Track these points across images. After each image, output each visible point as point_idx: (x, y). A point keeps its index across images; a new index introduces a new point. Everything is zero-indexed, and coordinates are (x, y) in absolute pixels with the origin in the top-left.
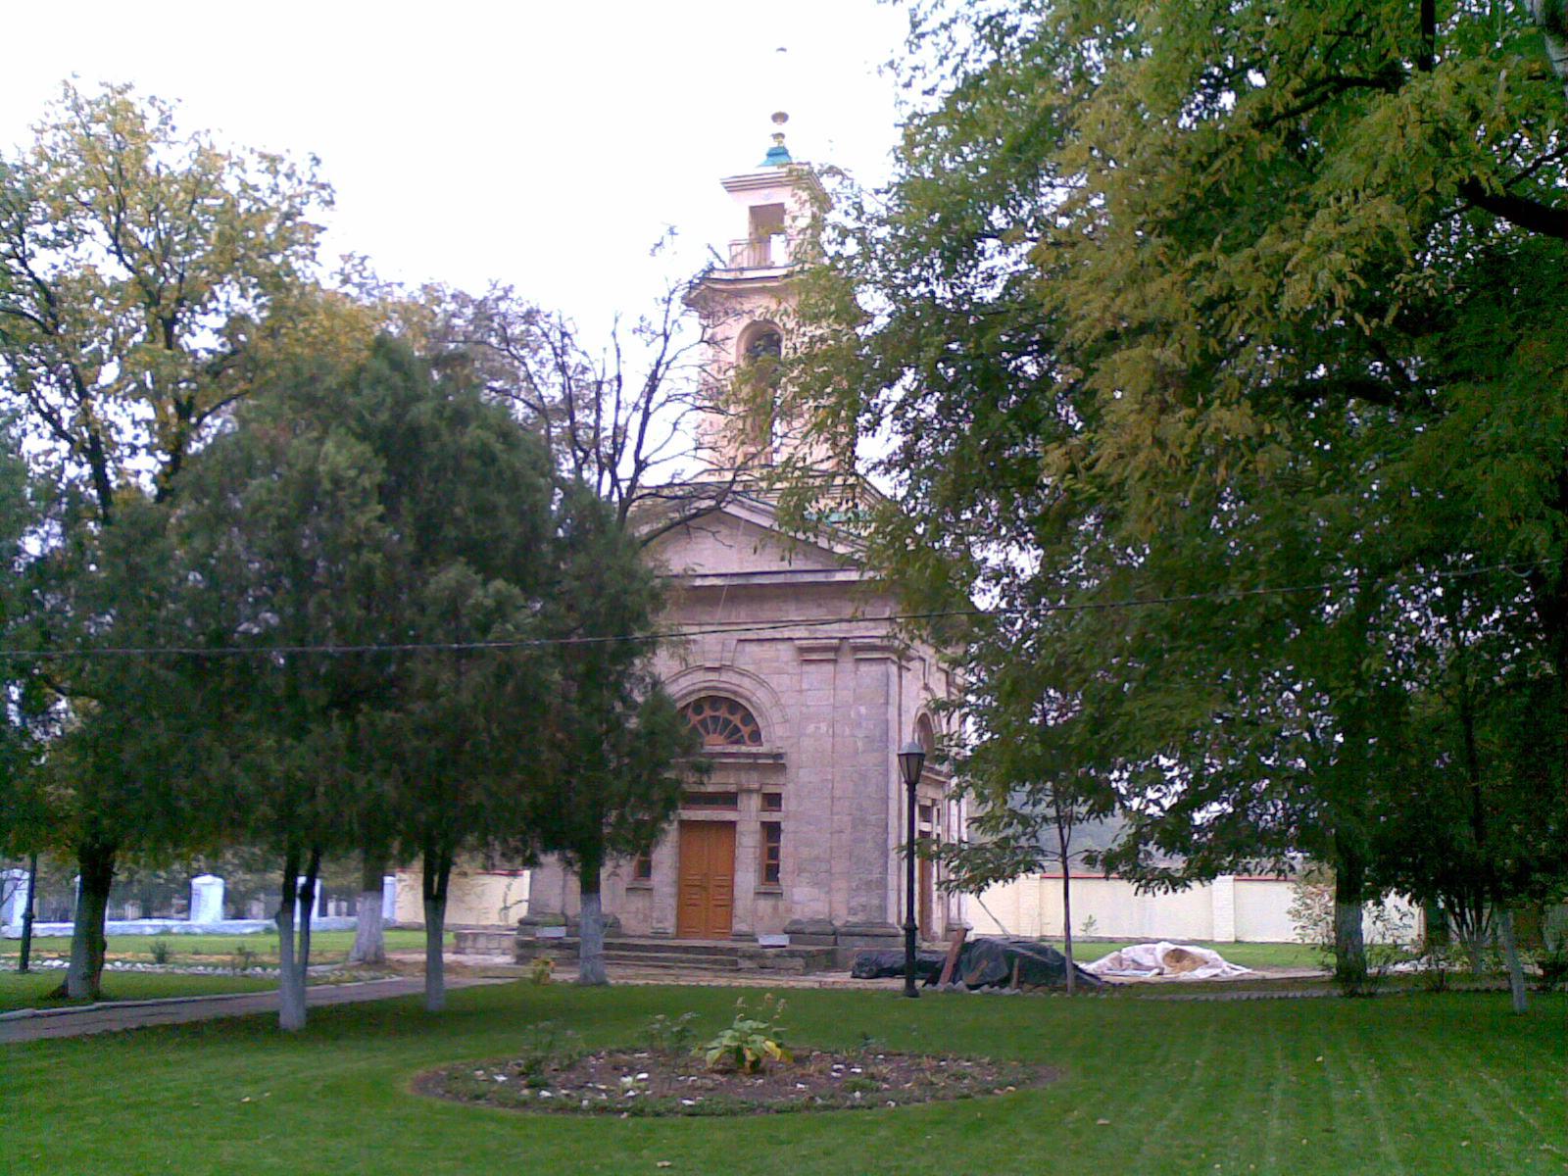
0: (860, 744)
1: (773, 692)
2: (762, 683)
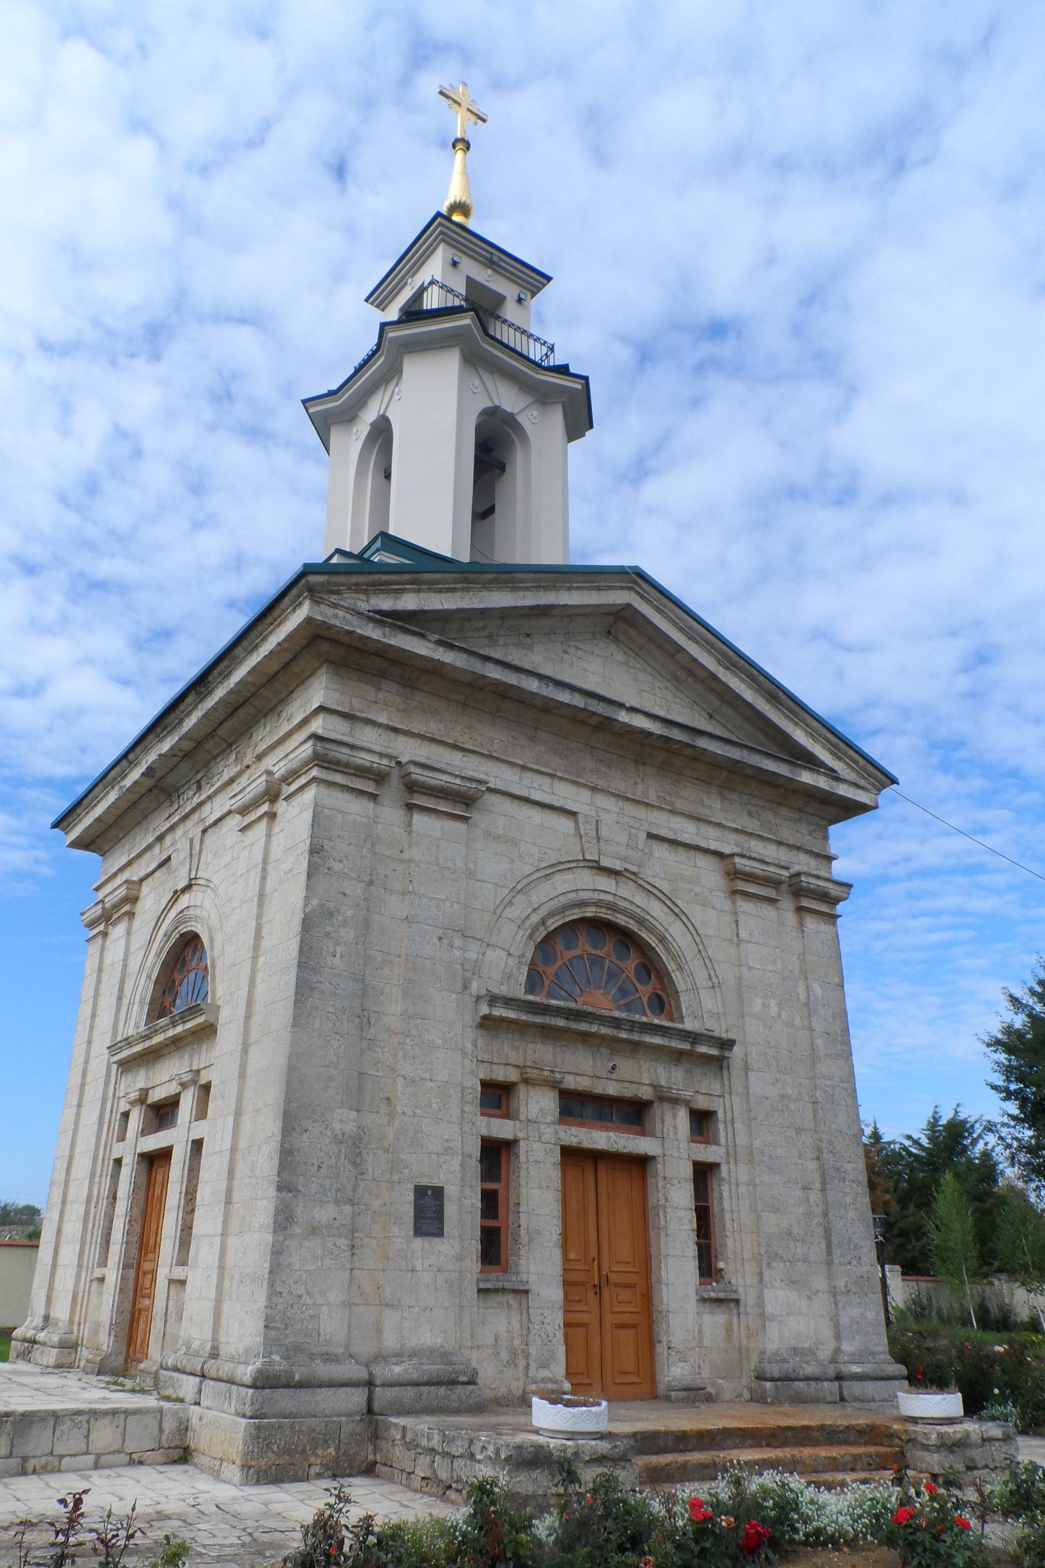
1: (694, 932)
2: (678, 914)
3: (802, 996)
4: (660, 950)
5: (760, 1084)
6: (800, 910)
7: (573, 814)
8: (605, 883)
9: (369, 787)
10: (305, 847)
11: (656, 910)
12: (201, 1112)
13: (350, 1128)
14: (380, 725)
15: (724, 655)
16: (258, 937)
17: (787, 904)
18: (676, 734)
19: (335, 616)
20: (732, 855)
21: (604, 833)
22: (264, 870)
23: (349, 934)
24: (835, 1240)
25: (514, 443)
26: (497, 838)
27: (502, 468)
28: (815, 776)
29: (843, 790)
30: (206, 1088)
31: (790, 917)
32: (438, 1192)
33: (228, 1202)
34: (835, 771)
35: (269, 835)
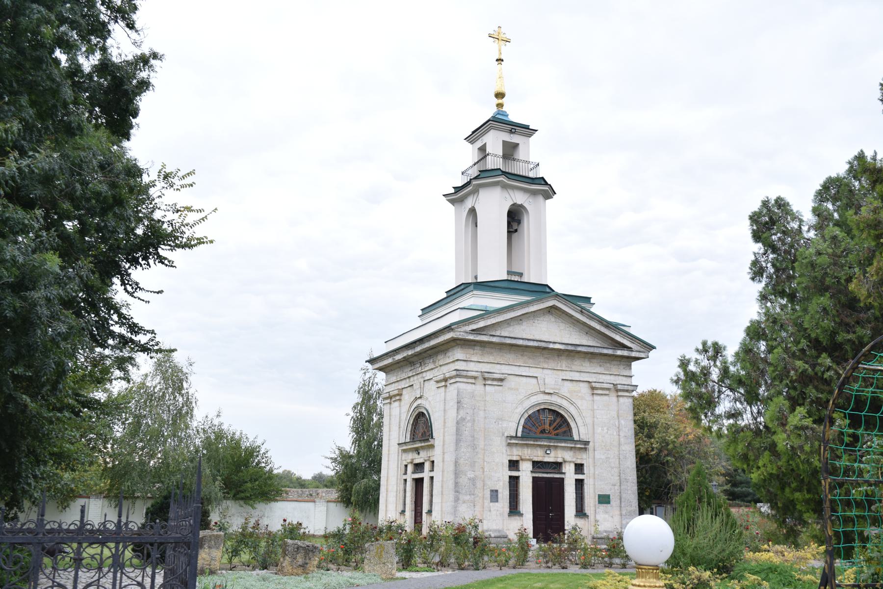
0: (622, 440)
1: (577, 408)
3: (617, 425)
4: (566, 416)
5: (598, 455)
6: (618, 396)
7: (536, 377)
8: (547, 397)
9: (473, 381)
10: (456, 401)
11: (565, 403)
12: (432, 470)
13: (472, 476)
14: (475, 361)
15: (588, 315)
16: (445, 422)
17: (613, 395)
18: (570, 348)
19: (460, 335)
20: (591, 382)
21: (546, 382)
22: (445, 402)
23: (469, 425)
24: (623, 500)
25: (523, 213)
26: (512, 389)
27: (519, 222)
28: (623, 351)
29: (634, 354)
30: (433, 462)
31: (614, 399)
32: (497, 491)
33: (442, 494)
34: (631, 348)
35: (445, 392)
